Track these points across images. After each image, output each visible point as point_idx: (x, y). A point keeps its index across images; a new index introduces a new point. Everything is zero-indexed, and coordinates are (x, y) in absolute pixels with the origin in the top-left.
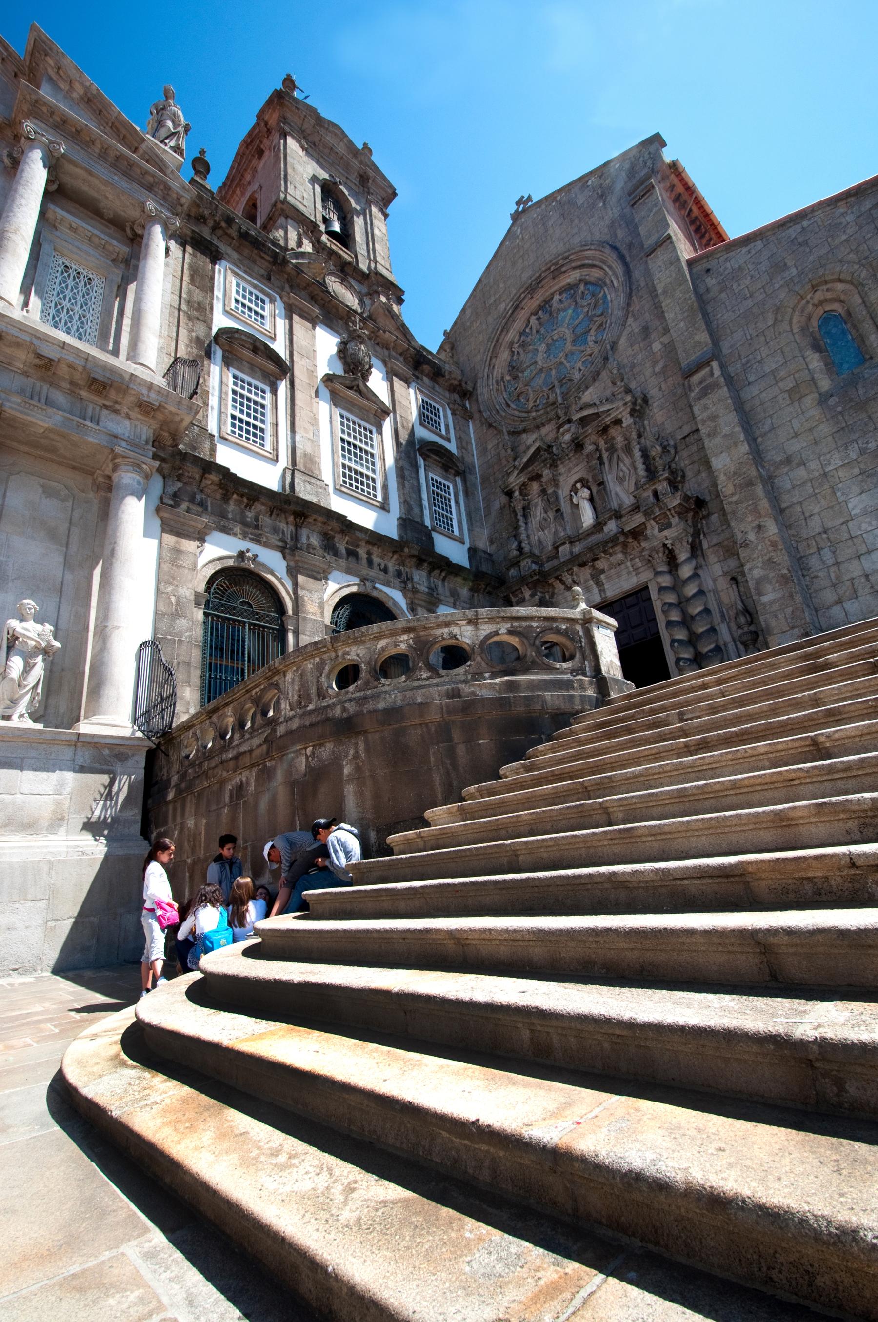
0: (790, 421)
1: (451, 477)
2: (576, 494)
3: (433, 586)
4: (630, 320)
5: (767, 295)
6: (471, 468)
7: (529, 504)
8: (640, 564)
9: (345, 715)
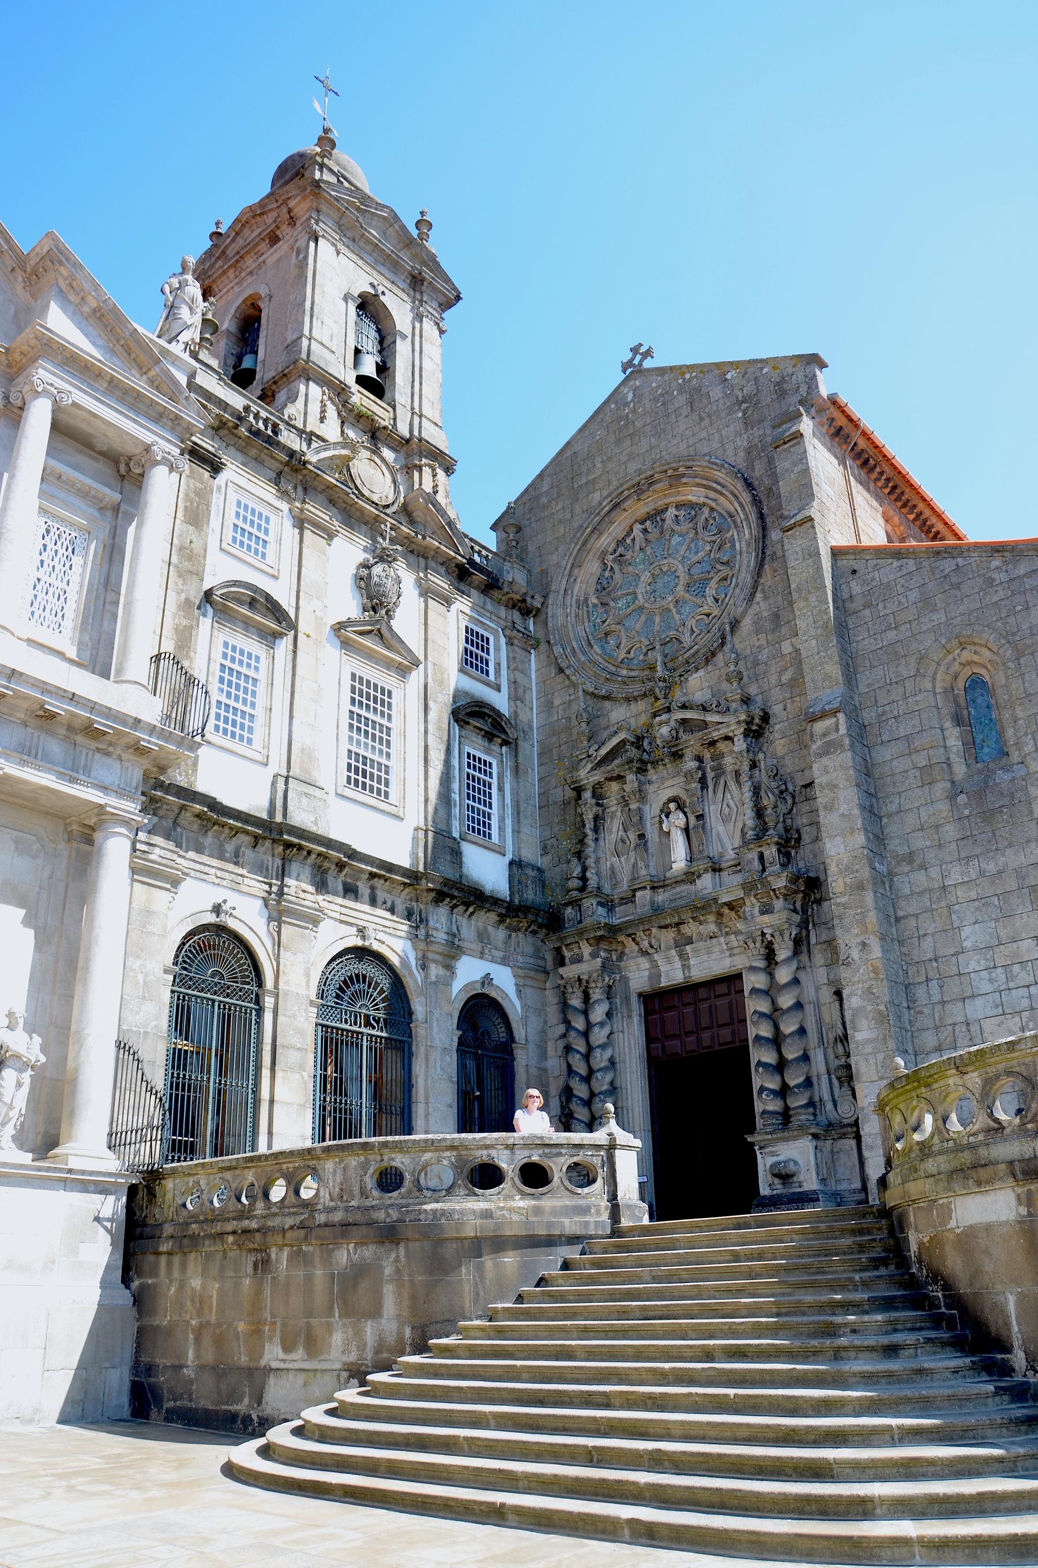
0: (918, 808)
1: (496, 748)
2: (667, 816)
3: (455, 930)
4: (759, 596)
5: (913, 635)
6: (527, 733)
7: (604, 811)
8: (735, 944)
9: (388, 1220)
